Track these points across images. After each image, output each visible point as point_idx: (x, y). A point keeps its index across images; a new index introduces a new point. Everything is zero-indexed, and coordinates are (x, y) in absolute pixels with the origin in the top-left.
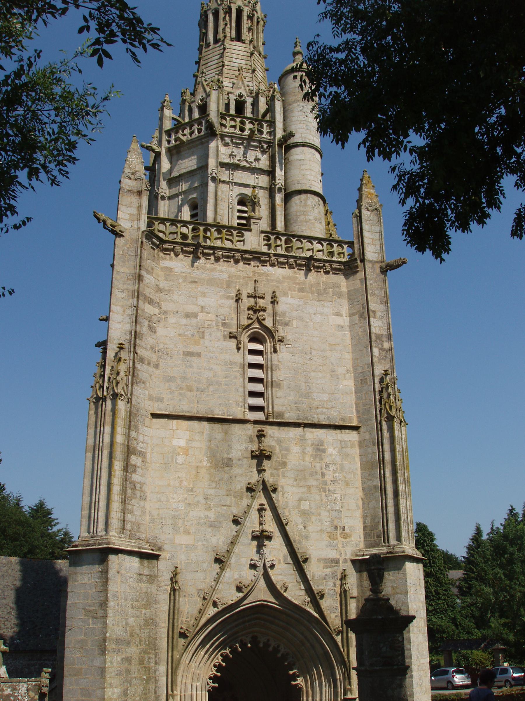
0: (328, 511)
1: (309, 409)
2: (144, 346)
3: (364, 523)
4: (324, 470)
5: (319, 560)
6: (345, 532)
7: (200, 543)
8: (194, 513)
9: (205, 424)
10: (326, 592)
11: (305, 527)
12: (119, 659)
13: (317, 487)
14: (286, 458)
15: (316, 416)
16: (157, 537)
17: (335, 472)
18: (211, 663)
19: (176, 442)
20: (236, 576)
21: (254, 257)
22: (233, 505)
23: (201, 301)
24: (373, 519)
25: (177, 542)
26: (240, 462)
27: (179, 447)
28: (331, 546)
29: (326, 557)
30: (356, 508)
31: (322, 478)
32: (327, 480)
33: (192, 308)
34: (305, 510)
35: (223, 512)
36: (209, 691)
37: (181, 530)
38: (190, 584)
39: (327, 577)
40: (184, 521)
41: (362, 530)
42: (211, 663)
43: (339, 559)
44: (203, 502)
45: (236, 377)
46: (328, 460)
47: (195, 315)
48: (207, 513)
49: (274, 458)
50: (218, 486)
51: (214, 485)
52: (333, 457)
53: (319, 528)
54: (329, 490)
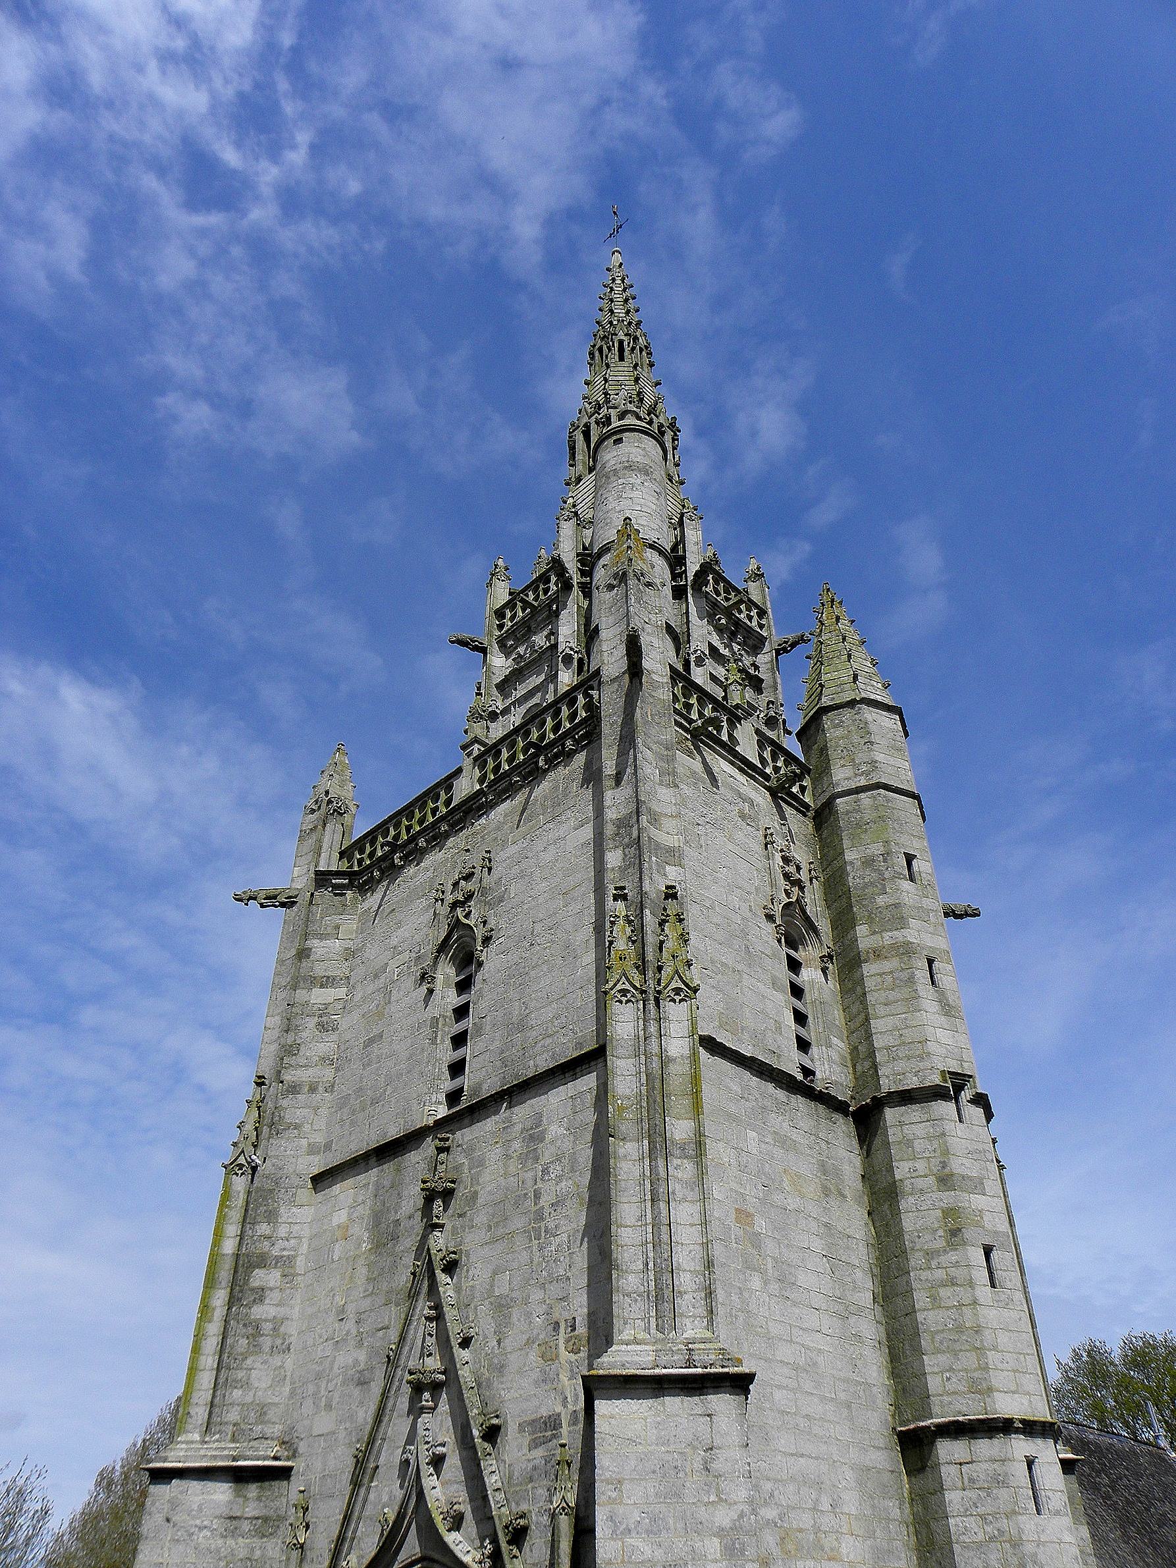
2: (303, 1061)
4: (540, 1185)
6: (576, 1332)
11: (499, 1342)
19: (335, 1222)
29: (533, 1417)
43: (559, 1415)
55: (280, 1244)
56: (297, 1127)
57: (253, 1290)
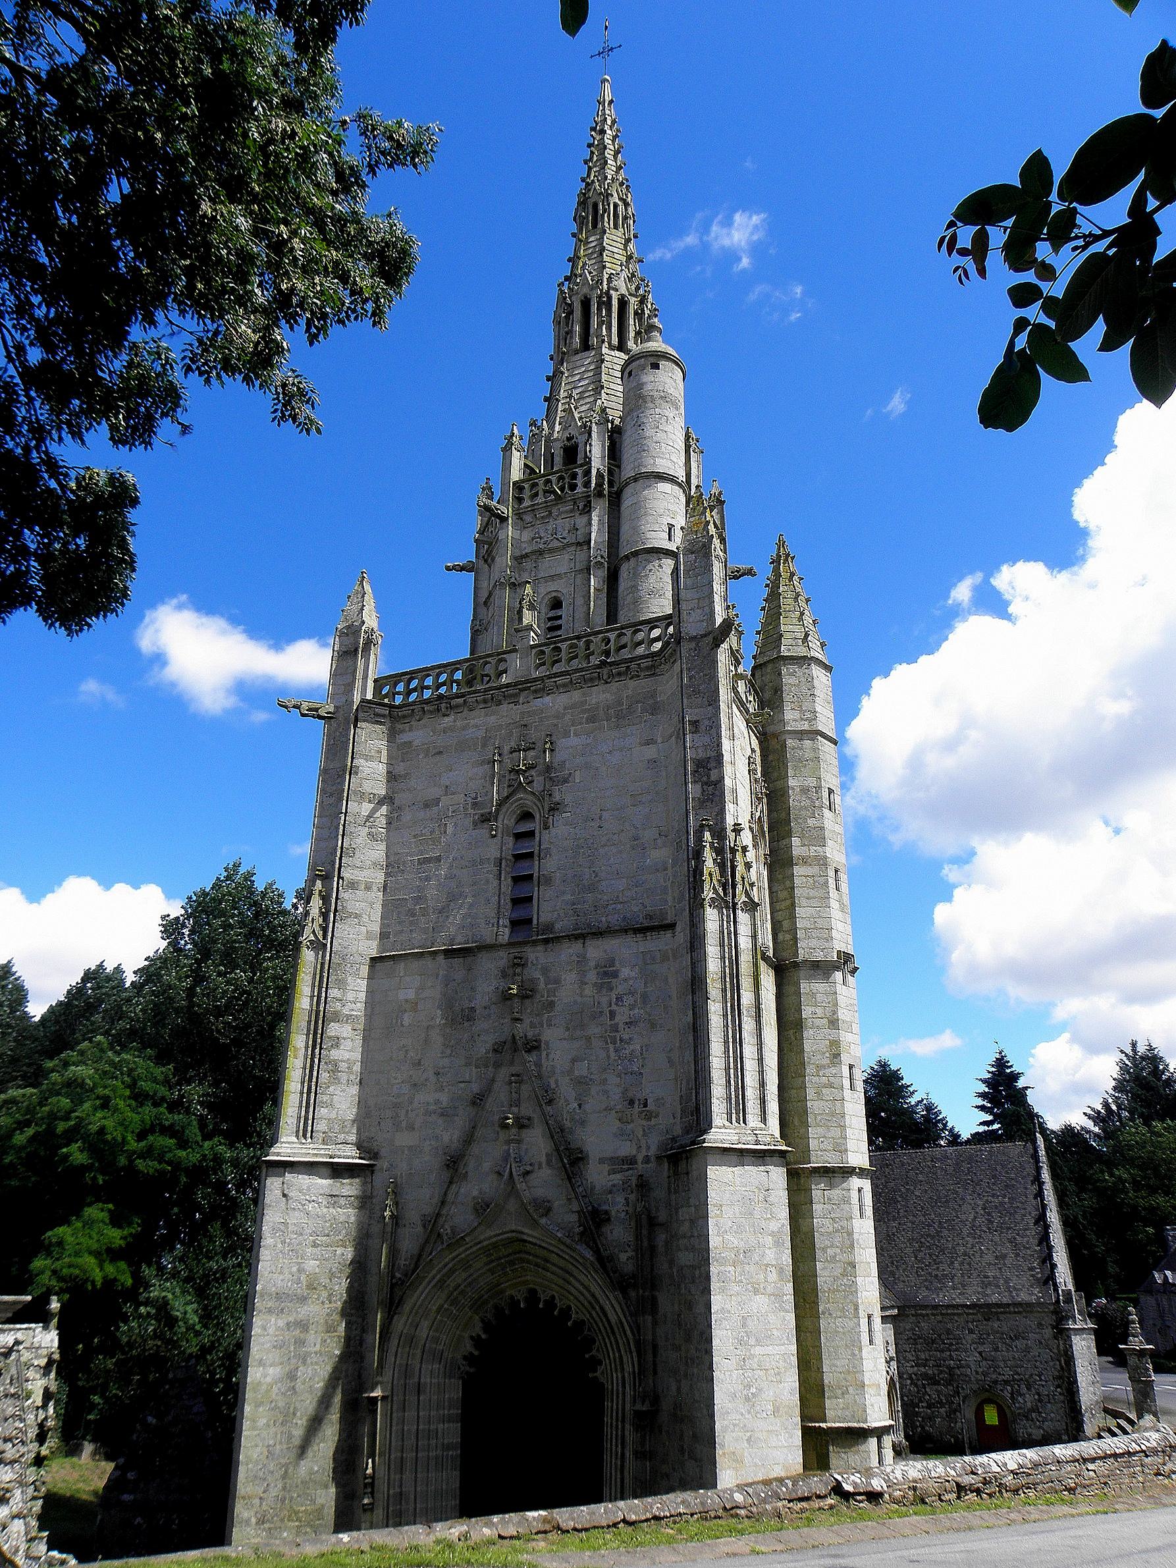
0: (619, 1076)
1: (593, 909)
4: (614, 1007)
5: (602, 1161)
8: (422, 1097)
11: (580, 1106)
12: (281, 1323)
14: (555, 996)
15: (604, 919)
19: (402, 995)
20: (475, 1193)
21: (521, 690)
23: (445, 781)
25: (397, 1143)
27: (406, 1001)
29: (613, 1155)
32: (618, 1024)
33: (434, 792)
37: (404, 1124)
39: (614, 1189)
44: (433, 1078)
45: (488, 881)
46: (620, 989)
47: (437, 801)
48: (437, 1096)
54: (621, 1040)
56: (357, 916)
57: (330, 1037)
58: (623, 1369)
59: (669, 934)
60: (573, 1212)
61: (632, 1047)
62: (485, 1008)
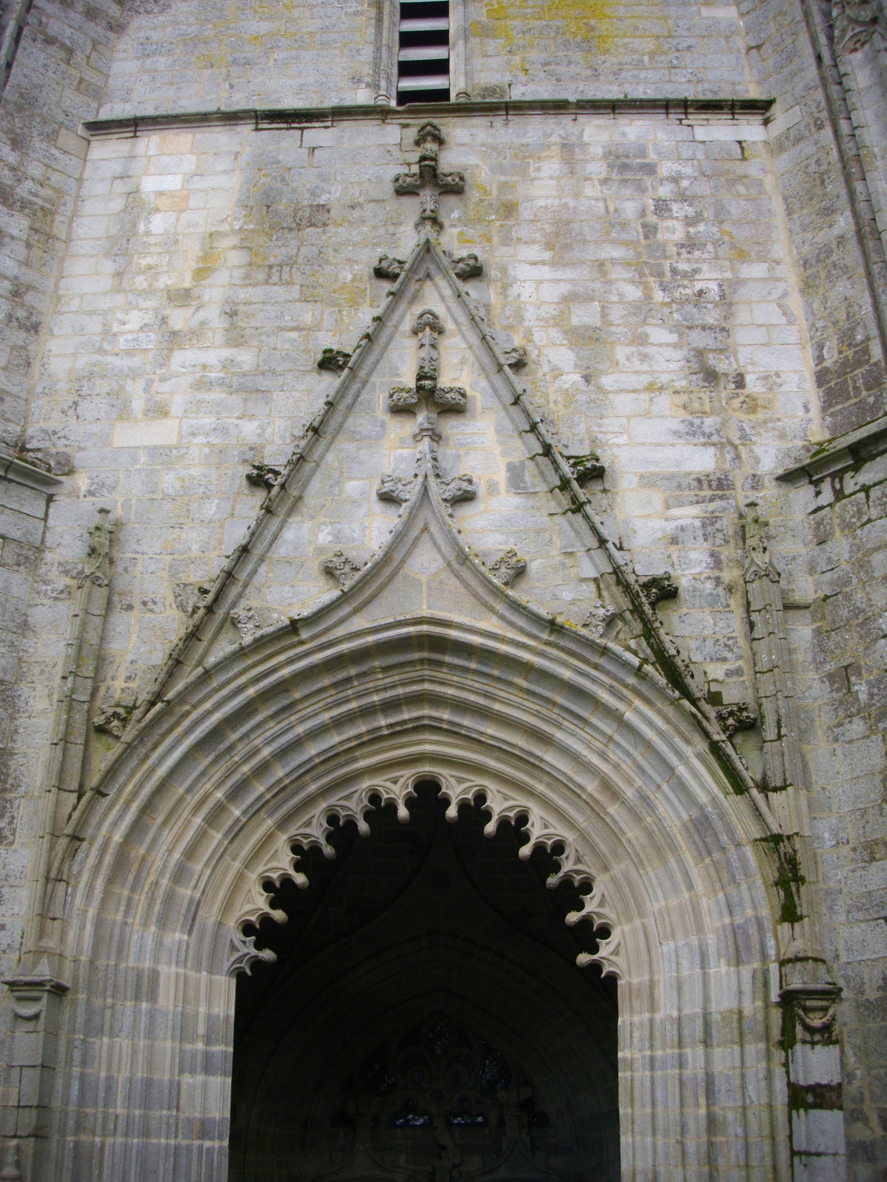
3: (820, 359)
4: (652, 219)
5: (648, 481)
6: (746, 391)
7: (200, 439)
9: (246, 129)
10: (683, 581)
11: (587, 379)
13: (629, 264)
16: (55, 433)
17: (691, 221)
18: (249, 864)
20: (324, 537)
22: (325, 325)
24: (847, 337)
26: (356, 214)
27: (161, 194)
28: (694, 435)
29: (673, 470)
30: (783, 320)
31: (646, 237)
34: (587, 328)
35: (287, 346)
36: (240, 976)
37: (138, 405)
38: (153, 567)
40: (149, 383)
41: (810, 384)
42: (249, 864)
46: (665, 191)
48: (227, 353)
49: (473, 194)
50: (275, 279)
51: (261, 276)
52: (685, 183)
53: (644, 380)
54: (674, 271)
55: (29, 185)
58: (700, 928)
59: (757, 119)
60: (583, 580)
61: (698, 286)
62: (353, 207)
